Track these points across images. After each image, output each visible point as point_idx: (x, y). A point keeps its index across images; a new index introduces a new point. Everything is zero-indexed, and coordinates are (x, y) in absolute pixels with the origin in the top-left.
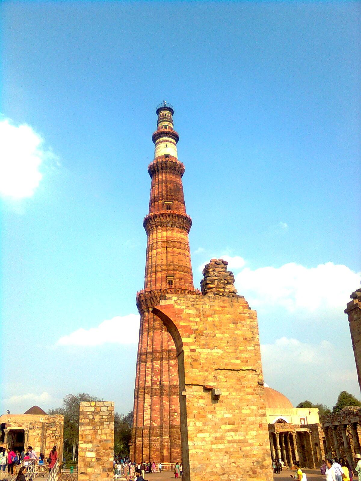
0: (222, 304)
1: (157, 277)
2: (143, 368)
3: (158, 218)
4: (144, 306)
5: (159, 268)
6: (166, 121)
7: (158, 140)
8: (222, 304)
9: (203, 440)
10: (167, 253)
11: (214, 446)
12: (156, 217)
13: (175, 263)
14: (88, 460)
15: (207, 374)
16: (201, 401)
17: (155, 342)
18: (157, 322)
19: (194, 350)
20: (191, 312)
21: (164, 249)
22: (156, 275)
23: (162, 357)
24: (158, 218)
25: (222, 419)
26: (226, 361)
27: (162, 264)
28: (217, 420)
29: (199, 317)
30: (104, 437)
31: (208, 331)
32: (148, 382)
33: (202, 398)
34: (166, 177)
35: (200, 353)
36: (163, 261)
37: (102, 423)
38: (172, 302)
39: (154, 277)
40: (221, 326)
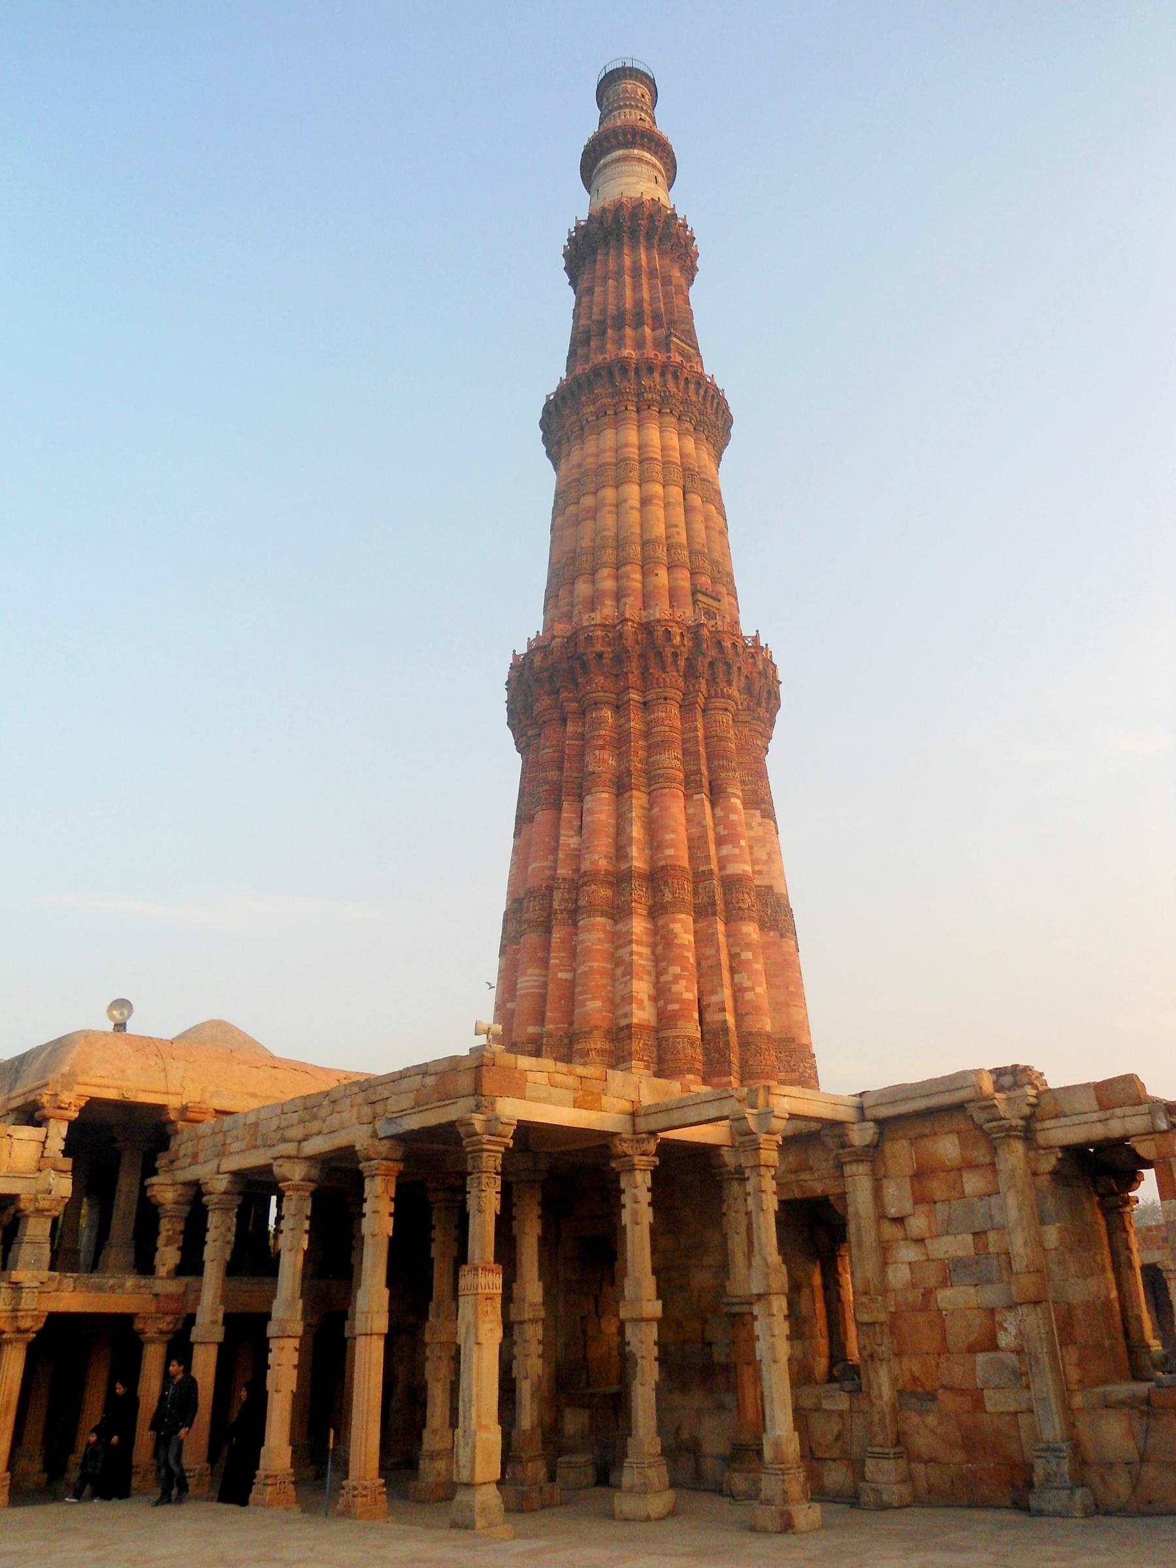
2: (599, 940)
3: (656, 375)
4: (601, 679)
5: (661, 553)
6: (647, 113)
7: (621, 152)
10: (688, 510)
12: (651, 370)
17: (672, 831)
18: (673, 754)
21: (676, 492)
23: (714, 904)
24: (656, 375)
27: (673, 540)
32: (641, 1007)
36: (678, 533)
39: (636, 581)
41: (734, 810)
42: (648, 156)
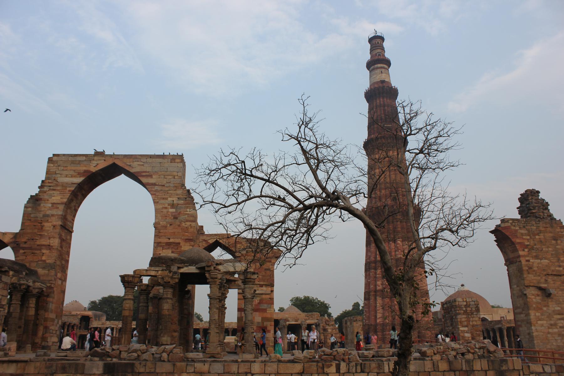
0: (544, 225)
1: (382, 194)
7: (372, 67)
8: (544, 225)
9: (542, 325)
11: (550, 330)
13: (397, 181)
14: (466, 339)
15: (539, 278)
16: (538, 298)
19: (528, 261)
20: (523, 231)
22: (380, 192)
25: (554, 311)
26: (553, 268)
28: (550, 312)
29: (529, 235)
30: (475, 323)
31: (538, 247)
33: (538, 295)
34: (383, 101)
35: (533, 263)
37: (472, 314)
38: (510, 224)
40: (546, 242)
41: (398, 244)
42: (379, 65)
